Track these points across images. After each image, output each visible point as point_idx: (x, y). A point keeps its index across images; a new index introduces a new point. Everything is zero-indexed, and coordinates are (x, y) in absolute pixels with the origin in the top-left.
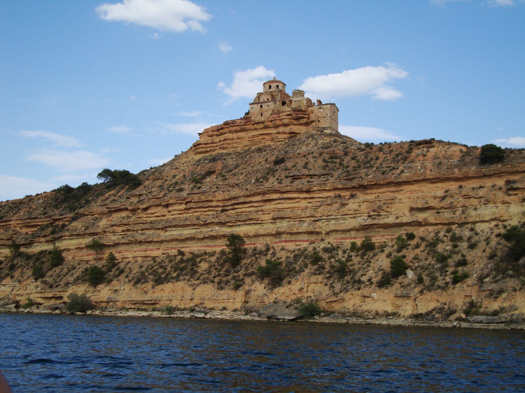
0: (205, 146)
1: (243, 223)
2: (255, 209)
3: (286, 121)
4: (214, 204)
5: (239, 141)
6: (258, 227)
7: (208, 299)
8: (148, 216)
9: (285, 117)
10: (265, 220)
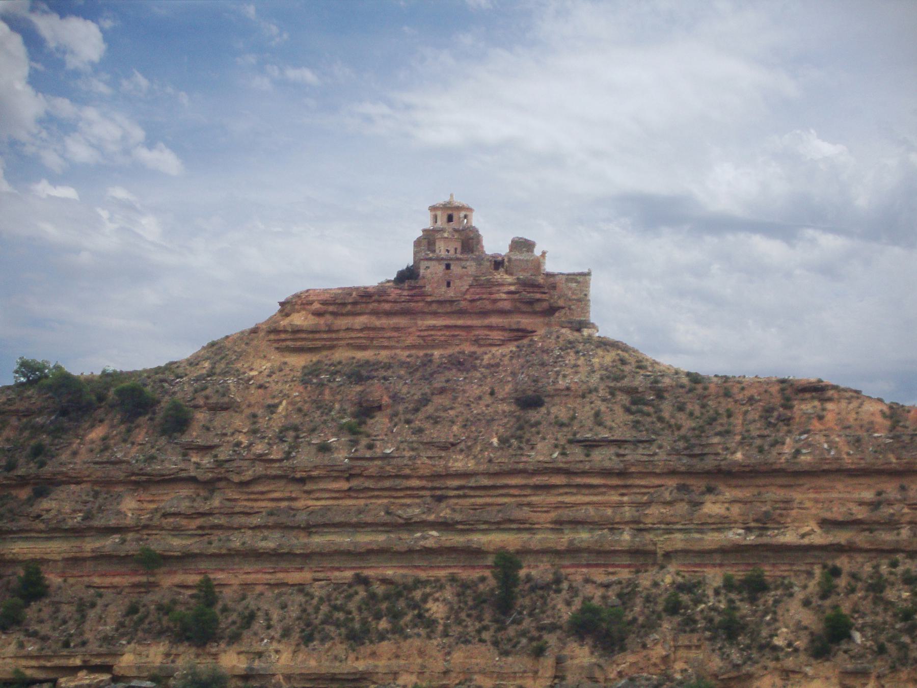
0: (311, 336)
1: (494, 527)
2: (513, 500)
3: (507, 305)
4: (415, 483)
5: (396, 334)
6: (525, 536)
7: (480, 672)
8: (252, 497)
9: (504, 296)
10: (538, 523)
